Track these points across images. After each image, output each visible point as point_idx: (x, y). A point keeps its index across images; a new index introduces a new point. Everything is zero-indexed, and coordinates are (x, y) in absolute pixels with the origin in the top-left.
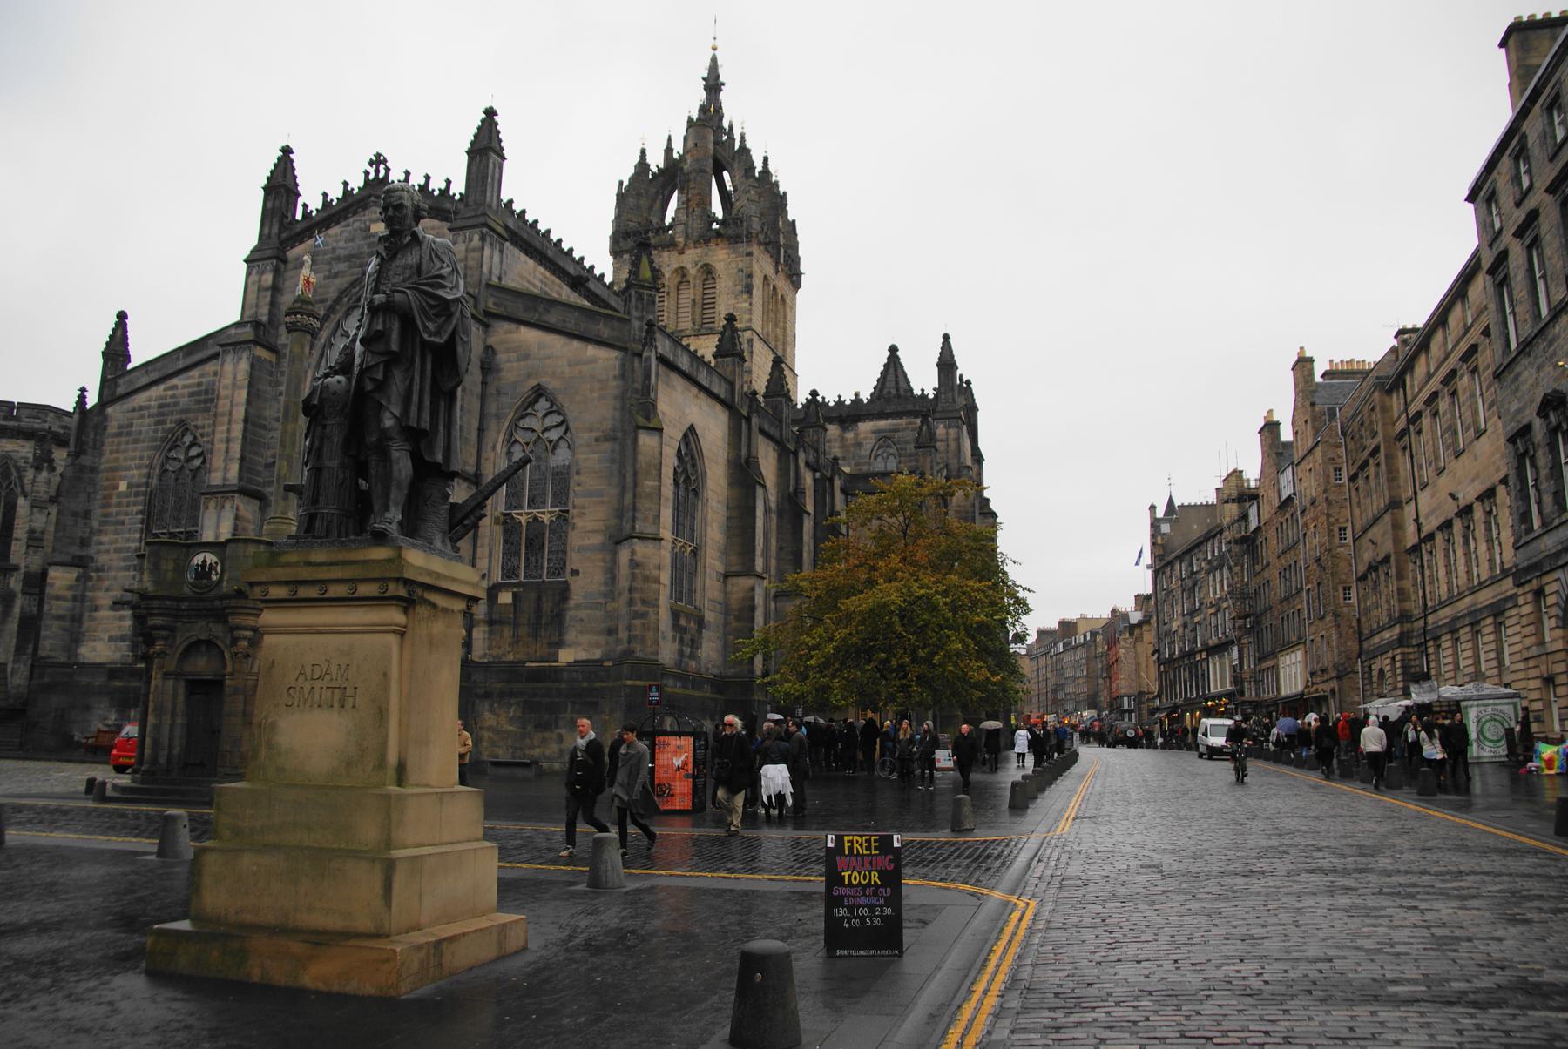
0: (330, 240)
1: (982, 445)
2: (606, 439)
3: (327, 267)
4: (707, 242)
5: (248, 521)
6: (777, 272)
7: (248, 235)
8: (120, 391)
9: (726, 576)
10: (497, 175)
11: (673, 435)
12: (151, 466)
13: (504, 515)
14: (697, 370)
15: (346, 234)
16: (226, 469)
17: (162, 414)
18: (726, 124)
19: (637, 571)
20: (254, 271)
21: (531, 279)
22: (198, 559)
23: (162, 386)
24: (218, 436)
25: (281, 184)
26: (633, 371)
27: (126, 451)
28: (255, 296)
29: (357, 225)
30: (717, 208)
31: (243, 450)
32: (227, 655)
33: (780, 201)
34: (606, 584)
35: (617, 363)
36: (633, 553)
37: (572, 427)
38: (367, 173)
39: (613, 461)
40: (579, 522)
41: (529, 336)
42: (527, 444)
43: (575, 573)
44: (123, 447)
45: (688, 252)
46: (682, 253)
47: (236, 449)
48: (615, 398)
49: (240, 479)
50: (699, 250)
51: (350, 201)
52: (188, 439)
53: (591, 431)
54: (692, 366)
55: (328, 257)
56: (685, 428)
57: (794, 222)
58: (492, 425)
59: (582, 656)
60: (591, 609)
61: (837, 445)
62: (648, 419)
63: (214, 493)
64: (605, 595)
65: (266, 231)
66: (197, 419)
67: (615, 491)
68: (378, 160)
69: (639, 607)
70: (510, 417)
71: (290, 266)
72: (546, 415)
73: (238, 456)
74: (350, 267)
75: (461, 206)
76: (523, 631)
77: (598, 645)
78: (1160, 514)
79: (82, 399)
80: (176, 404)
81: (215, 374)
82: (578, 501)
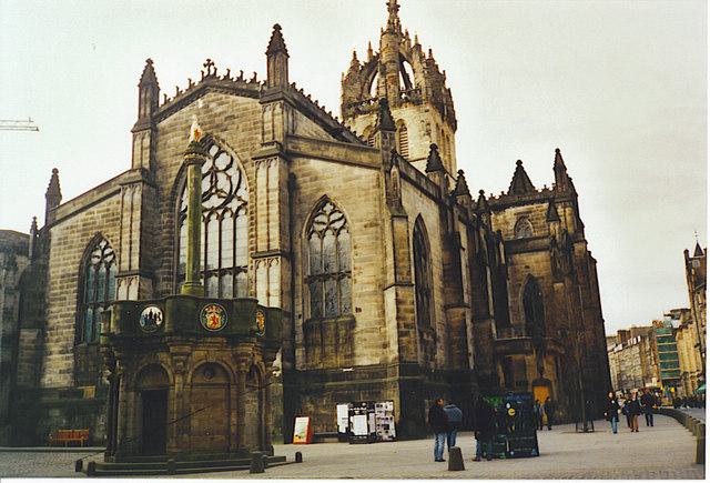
2: (371, 225)
7: (131, 115)
8: (58, 218)
9: (446, 308)
11: (412, 219)
12: (81, 262)
17: (85, 230)
18: (403, 31)
23: (84, 213)
25: (149, 82)
30: (402, 84)
33: (442, 78)
37: (349, 221)
40: (358, 278)
41: (315, 165)
49: (140, 266)
52: (103, 244)
67: (380, 257)
68: (209, 64)
69: (403, 329)
72: (331, 213)
75: (265, 88)
77: (377, 355)
78: (691, 255)
79: (35, 223)
82: (357, 265)
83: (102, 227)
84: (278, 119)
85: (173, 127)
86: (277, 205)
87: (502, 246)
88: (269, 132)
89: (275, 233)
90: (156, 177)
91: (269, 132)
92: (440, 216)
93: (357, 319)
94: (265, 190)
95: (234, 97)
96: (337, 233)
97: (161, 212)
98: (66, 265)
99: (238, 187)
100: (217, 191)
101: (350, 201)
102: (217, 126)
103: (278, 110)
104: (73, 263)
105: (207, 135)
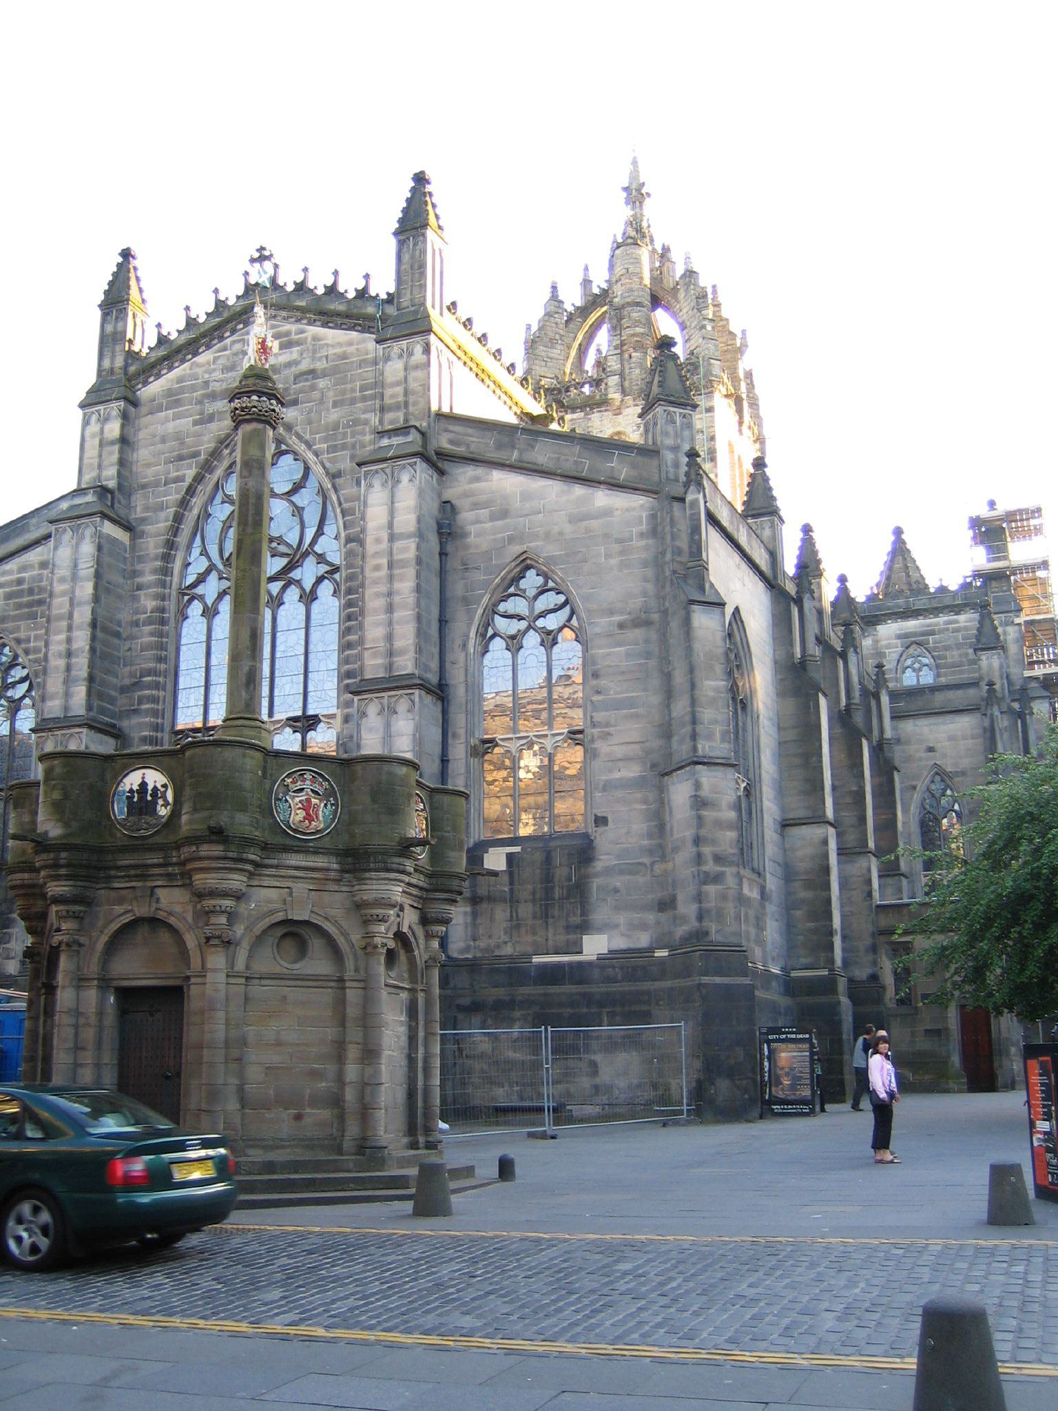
0: (199, 371)
3: (198, 407)
9: (785, 825)
16: (67, 695)
19: (705, 813)
20: (94, 418)
22: (132, 780)
24: (54, 648)
26: (673, 523)
28: (95, 453)
31: (91, 666)
32: (191, 941)
34: (650, 836)
36: (698, 785)
39: (648, 655)
42: (513, 637)
45: (626, 412)
46: (618, 412)
47: (81, 664)
48: (645, 564)
49: (89, 708)
51: (226, 315)
53: (611, 613)
59: (621, 943)
60: (630, 873)
62: (702, 588)
63: (50, 730)
64: (650, 852)
65: (107, 364)
66: (18, 629)
67: (655, 699)
68: (262, 257)
69: (710, 867)
70: (485, 600)
71: (143, 410)
73: (84, 673)
76: (526, 910)
77: (643, 926)
81: (44, 565)
85: (173, 399)
86: (411, 572)
87: (885, 699)
88: (397, 407)
89: (406, 636)
90: (129, 507)
91: (397, 407)
92: (773, 615)
94: (385, 535)
96: (550, 640)
97: (140, 587)
99: (320, 532)
100: (271, 540)
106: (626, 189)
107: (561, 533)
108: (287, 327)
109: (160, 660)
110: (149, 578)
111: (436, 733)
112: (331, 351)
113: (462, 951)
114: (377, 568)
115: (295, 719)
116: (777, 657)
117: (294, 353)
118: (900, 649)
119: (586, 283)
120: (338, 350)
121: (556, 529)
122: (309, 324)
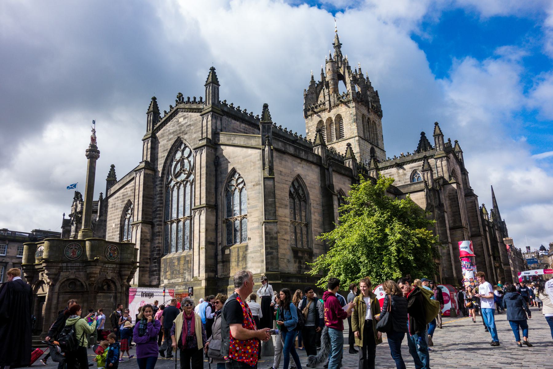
1: (467, 166)
4: (338, 105)
5: (147, 233)
6: (369, 112)
8: (112, 192)
10: (216, 92)
13: (227, 219)
14: (299, 153)
15: (172, 124)
21: (239, 129)
27: (114, 213)
29: (175, 120)
34: (260, 242)
35: (259, 154)
38: (177, 101)
39: (259, 193)
43: (250, 239)
44: (113, 212)
46: (329, 111)
49: (142, 218)
50: (335, 110)
53: (252, 182)
54: (295, 151)
55: (167, 134)
56: (295, 175)
57: (377, 91)
58: (220, 186)
60: (256, 253)
61: (396, 176)
69: (269, 250)
74: (174, 136)
77: (259, 267)
79: (101, 196)
80: (127, 194)
83: (130, 196)
84: (210, 123)
93: (249, 245)
95: (190, 114)
97: (156, 185)
98: (114, 219)
100: (184, 171)
101: (246, 170)
102: (183, 132)
103: (210, 118)
104: (118, 218)
105: (179, 137)
106: (334, 44)
107: (241, 162)
108: (185, 113)
109: (161, 203)
110: (158, 183)
111: (213, 218)
112: (194, 119)
113: (220, 276)
114: (198, 176)
115: (189, 217)
116: (322, 186)
117: (186, 121)
118: (411, 172)
119: (323, 74)
120: (195, 118)
121: (240, 161)
122: (190, 112)
